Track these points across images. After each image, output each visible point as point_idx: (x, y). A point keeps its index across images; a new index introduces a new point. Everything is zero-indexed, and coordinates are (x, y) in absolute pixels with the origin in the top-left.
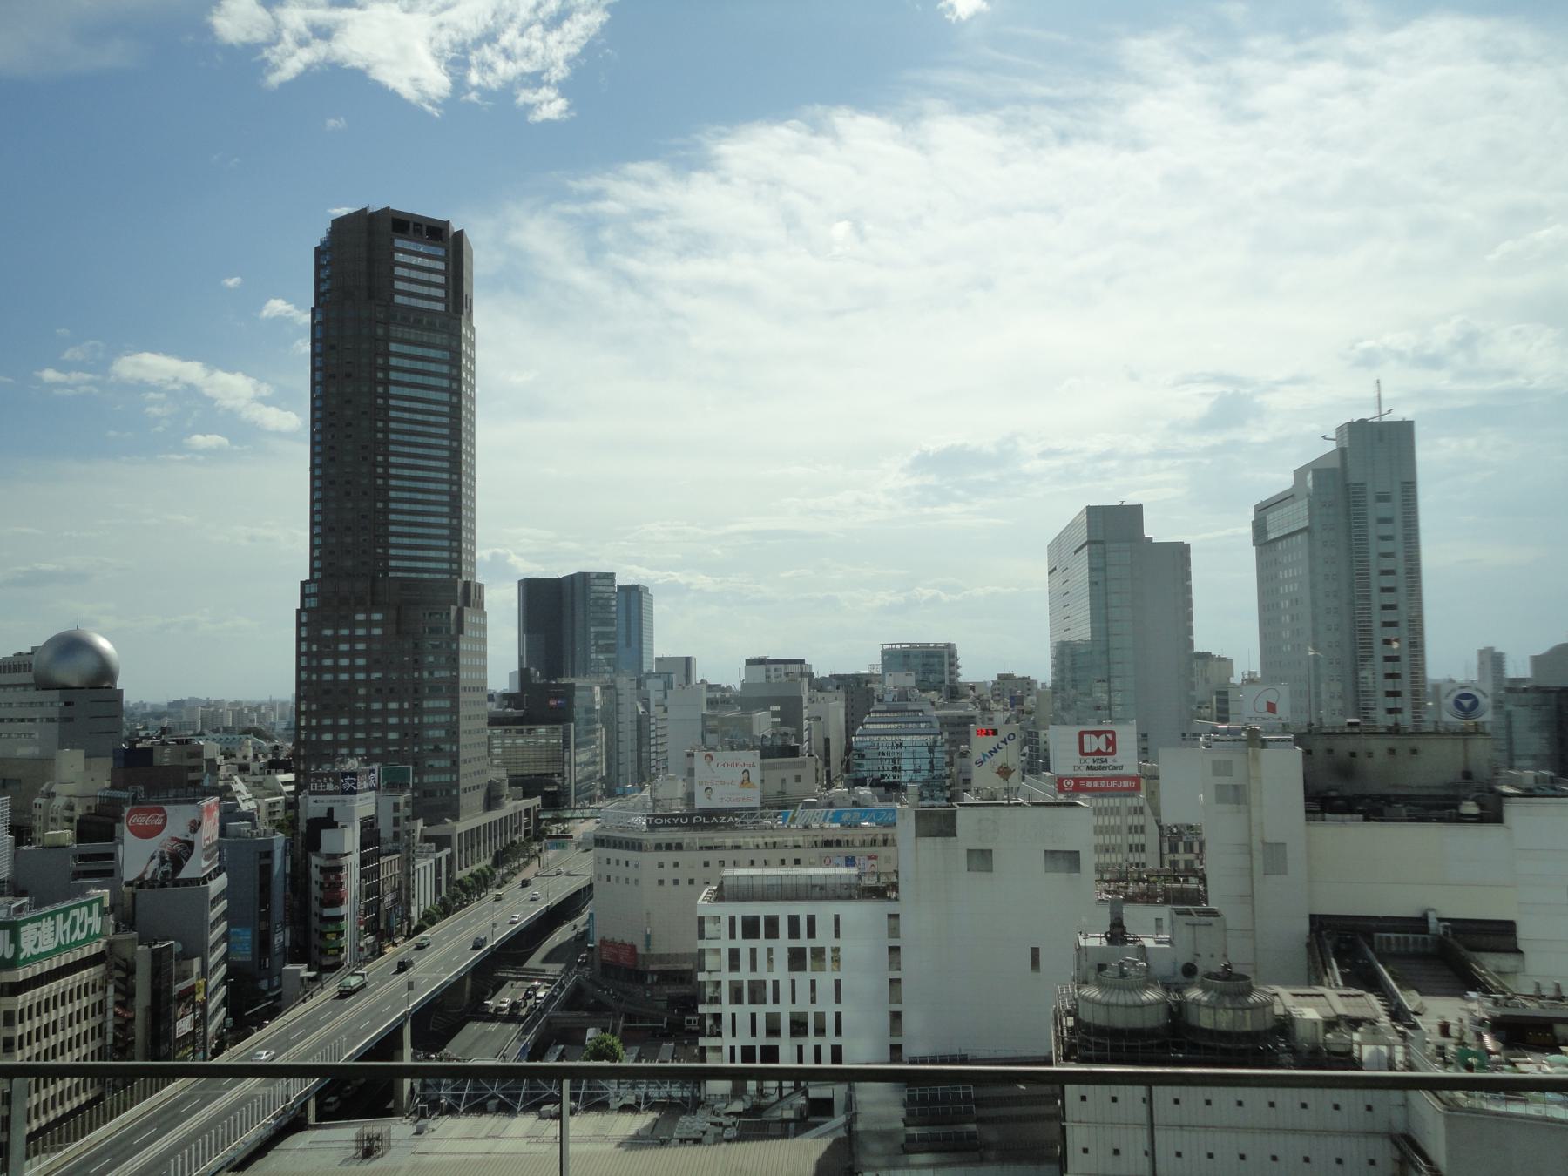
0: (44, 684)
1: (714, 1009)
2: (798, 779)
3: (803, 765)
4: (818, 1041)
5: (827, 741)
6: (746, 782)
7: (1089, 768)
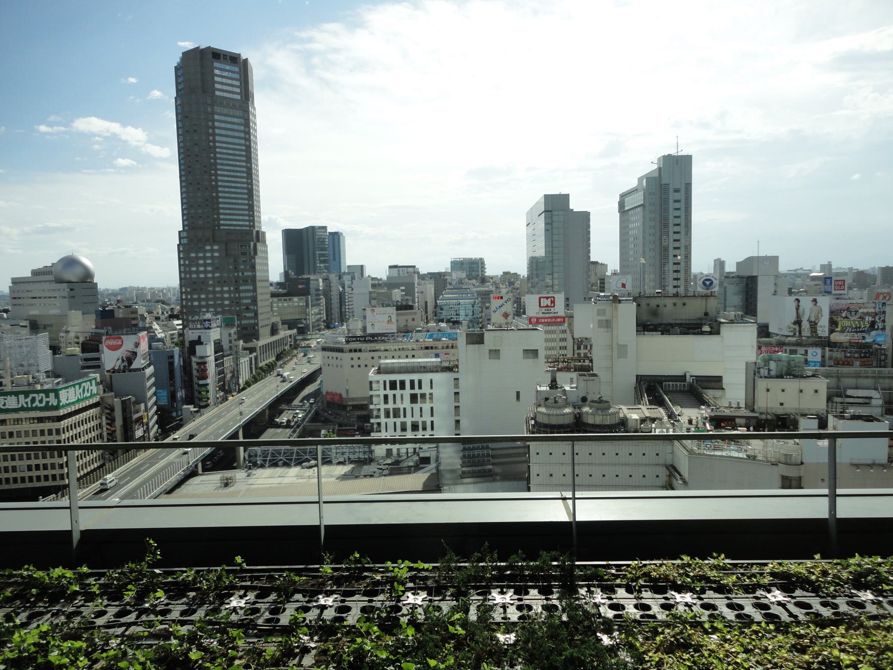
0: (60, 281)
2: (413, 320)
3: (415, 313)
5: (426, 302)
6: (390, 321)
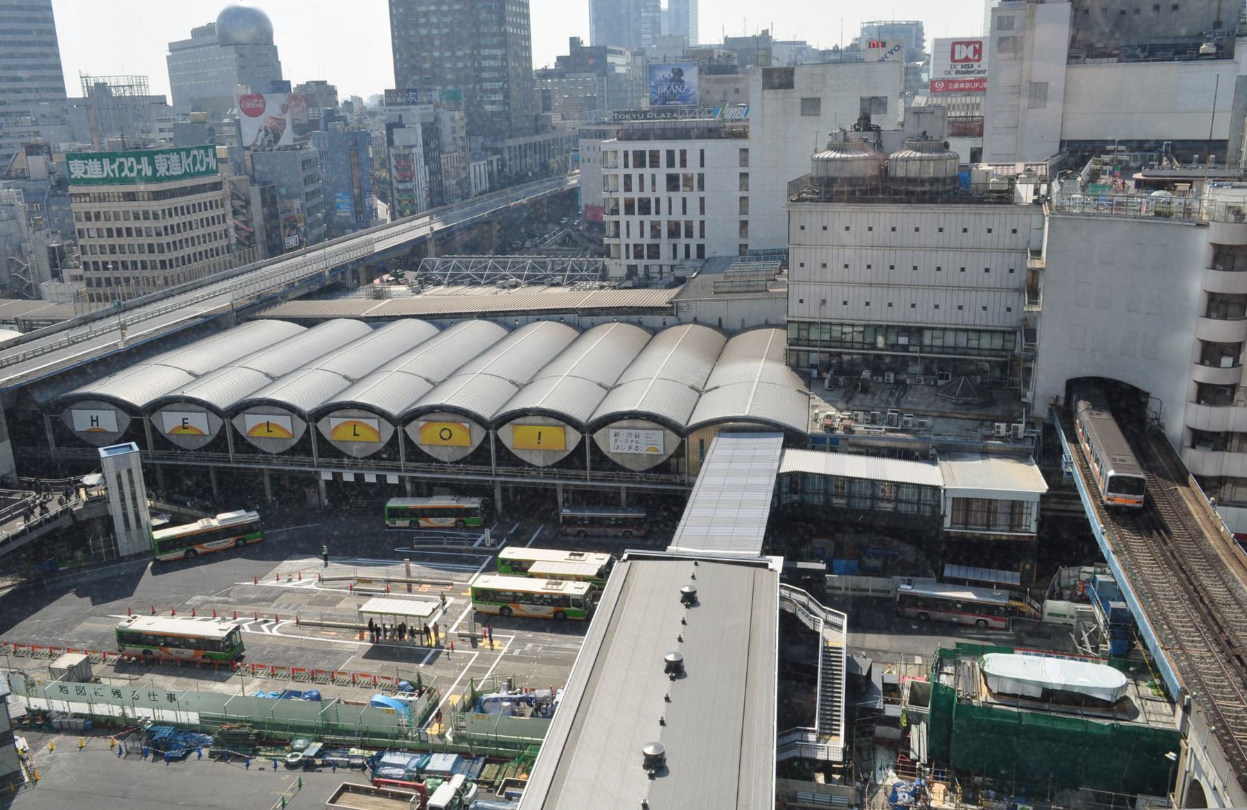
0: (225, 41)
1: (615, 218)
4: (687, 241)
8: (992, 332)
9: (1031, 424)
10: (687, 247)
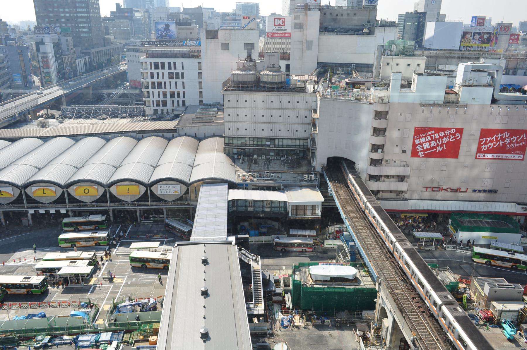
1: (147, 90)
2: (191, 33)
4: (178, 99)
7: (276, 30)
8: (300, 139)
9: (316, 175)
10: (178, 102)
